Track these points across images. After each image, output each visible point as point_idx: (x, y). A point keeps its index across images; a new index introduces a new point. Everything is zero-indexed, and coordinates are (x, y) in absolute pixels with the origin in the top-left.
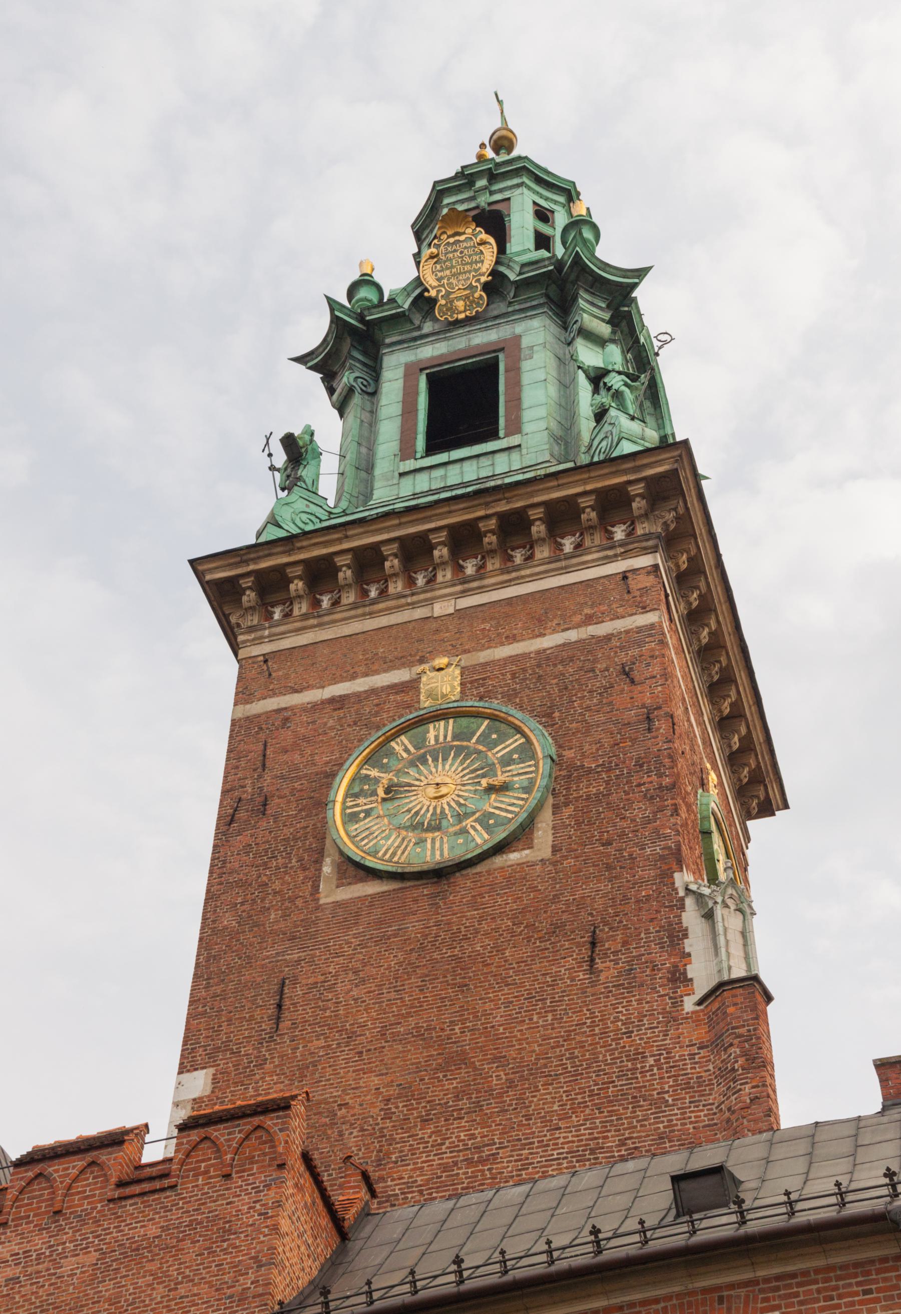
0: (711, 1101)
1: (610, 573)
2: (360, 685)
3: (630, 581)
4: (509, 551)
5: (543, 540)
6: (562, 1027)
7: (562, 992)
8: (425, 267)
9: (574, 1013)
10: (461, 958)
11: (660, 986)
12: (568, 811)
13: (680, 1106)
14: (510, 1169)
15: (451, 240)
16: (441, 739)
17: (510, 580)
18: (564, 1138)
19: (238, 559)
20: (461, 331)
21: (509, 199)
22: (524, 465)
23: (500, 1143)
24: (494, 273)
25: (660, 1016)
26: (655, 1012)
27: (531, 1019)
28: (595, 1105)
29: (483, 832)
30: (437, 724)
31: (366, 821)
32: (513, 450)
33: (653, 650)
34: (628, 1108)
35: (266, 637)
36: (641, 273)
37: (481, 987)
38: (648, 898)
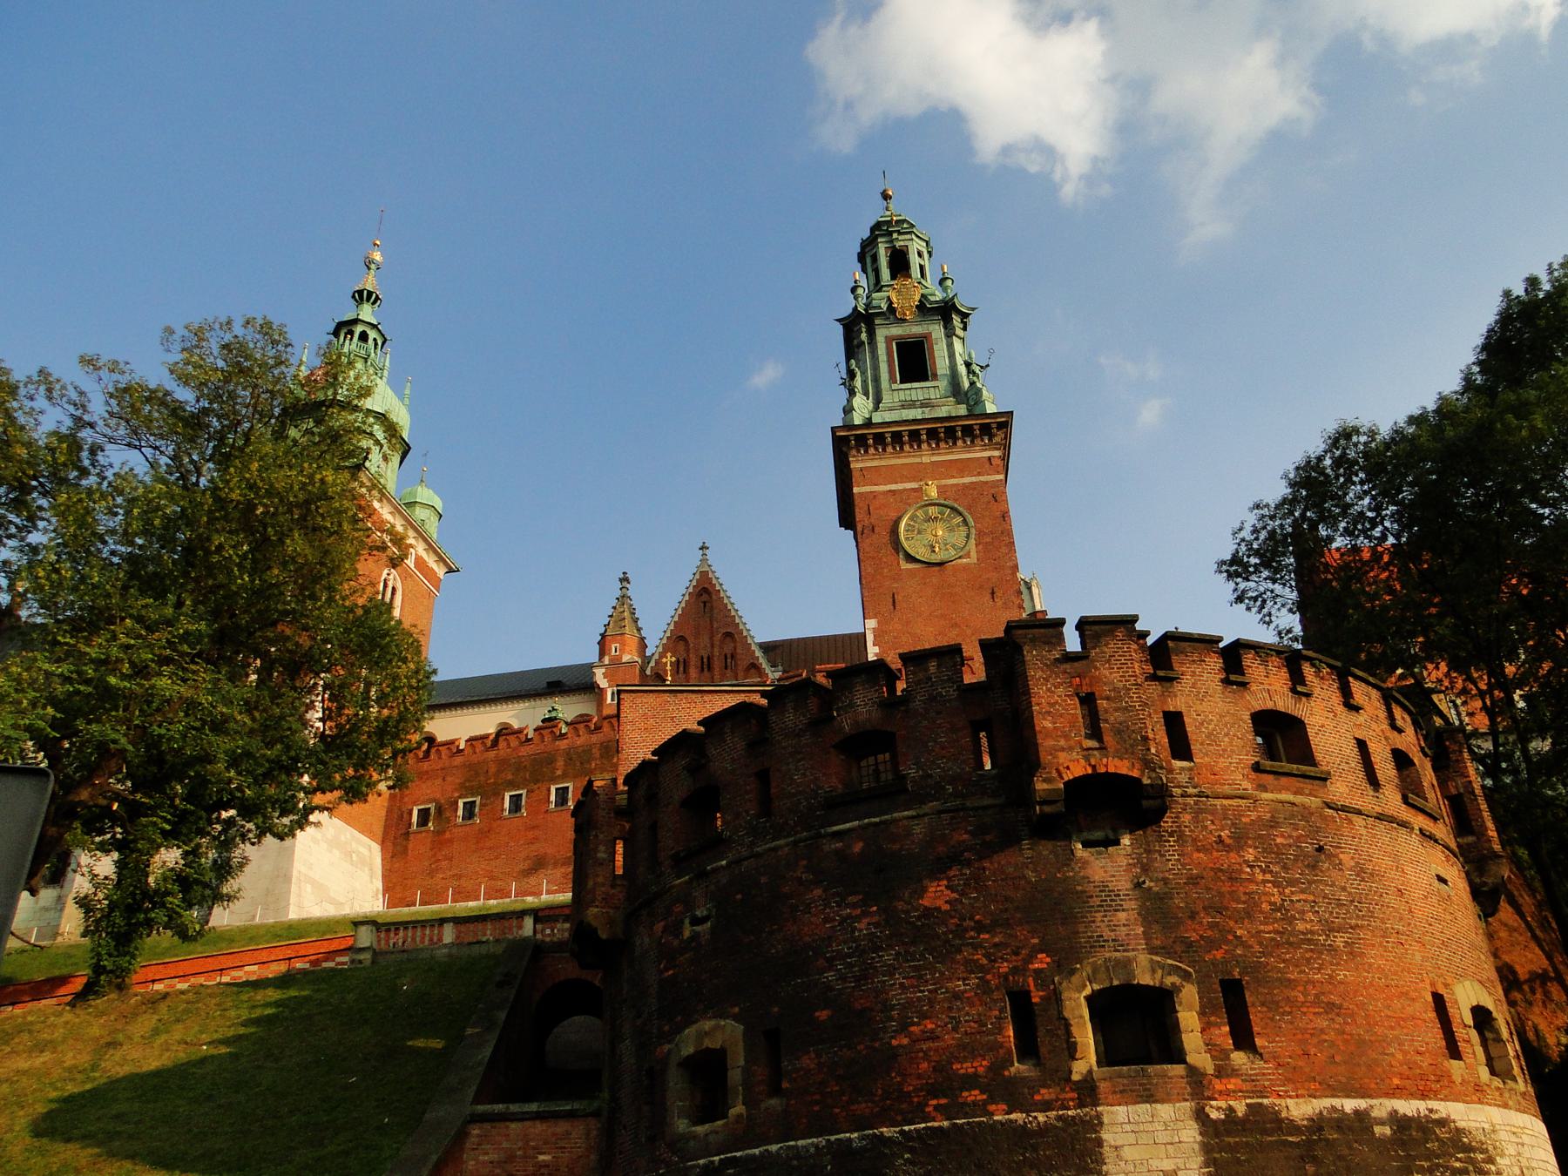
12: (981, 547)
24: (920, 301)
36: (973, 309)
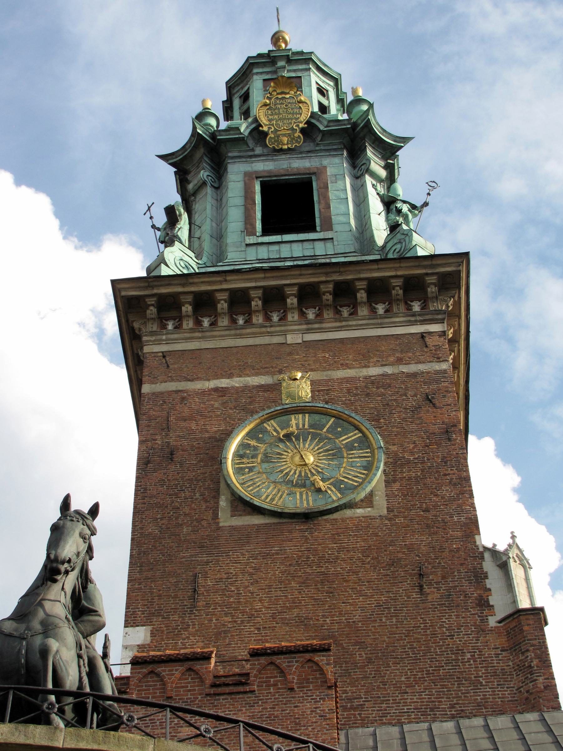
0: (512, 685)
1: (413, 332)
2: (236, 382)
3: (427, 339)
4: (338, 307)
5: (365, 303)
6: (403, 627)
7: (402, 604)
8: (260, 111)
9: (412, 619)
10: (326, 574)
11: (471, 608)
12: (396, 486)
13: (491, 686)
14: (374, 715)
15: (280, 96)
16: (301, 426)
17: (342, 327)
18: (411, 699)
19: (146, 284)
20: (283, 157)
21: (300, 77)
22: (336, 252)
23: (365, 698)
24: (308, 123)
25: (473, 627)
26: (469, 625)
27: (381, 620)
28: (431, 680)
29: (337, 492)
30: (297, 416)
31: (251, 474)
32: (327, 241)
33: (447, 387)
34: (454, 684)
35: (163, 340)
36: (405, 140)
37: (343, 595)
38: (458, 550)
